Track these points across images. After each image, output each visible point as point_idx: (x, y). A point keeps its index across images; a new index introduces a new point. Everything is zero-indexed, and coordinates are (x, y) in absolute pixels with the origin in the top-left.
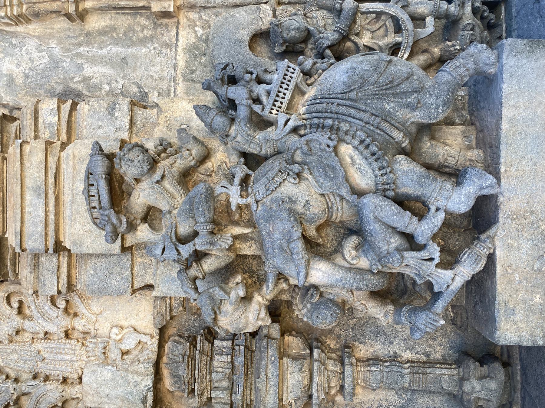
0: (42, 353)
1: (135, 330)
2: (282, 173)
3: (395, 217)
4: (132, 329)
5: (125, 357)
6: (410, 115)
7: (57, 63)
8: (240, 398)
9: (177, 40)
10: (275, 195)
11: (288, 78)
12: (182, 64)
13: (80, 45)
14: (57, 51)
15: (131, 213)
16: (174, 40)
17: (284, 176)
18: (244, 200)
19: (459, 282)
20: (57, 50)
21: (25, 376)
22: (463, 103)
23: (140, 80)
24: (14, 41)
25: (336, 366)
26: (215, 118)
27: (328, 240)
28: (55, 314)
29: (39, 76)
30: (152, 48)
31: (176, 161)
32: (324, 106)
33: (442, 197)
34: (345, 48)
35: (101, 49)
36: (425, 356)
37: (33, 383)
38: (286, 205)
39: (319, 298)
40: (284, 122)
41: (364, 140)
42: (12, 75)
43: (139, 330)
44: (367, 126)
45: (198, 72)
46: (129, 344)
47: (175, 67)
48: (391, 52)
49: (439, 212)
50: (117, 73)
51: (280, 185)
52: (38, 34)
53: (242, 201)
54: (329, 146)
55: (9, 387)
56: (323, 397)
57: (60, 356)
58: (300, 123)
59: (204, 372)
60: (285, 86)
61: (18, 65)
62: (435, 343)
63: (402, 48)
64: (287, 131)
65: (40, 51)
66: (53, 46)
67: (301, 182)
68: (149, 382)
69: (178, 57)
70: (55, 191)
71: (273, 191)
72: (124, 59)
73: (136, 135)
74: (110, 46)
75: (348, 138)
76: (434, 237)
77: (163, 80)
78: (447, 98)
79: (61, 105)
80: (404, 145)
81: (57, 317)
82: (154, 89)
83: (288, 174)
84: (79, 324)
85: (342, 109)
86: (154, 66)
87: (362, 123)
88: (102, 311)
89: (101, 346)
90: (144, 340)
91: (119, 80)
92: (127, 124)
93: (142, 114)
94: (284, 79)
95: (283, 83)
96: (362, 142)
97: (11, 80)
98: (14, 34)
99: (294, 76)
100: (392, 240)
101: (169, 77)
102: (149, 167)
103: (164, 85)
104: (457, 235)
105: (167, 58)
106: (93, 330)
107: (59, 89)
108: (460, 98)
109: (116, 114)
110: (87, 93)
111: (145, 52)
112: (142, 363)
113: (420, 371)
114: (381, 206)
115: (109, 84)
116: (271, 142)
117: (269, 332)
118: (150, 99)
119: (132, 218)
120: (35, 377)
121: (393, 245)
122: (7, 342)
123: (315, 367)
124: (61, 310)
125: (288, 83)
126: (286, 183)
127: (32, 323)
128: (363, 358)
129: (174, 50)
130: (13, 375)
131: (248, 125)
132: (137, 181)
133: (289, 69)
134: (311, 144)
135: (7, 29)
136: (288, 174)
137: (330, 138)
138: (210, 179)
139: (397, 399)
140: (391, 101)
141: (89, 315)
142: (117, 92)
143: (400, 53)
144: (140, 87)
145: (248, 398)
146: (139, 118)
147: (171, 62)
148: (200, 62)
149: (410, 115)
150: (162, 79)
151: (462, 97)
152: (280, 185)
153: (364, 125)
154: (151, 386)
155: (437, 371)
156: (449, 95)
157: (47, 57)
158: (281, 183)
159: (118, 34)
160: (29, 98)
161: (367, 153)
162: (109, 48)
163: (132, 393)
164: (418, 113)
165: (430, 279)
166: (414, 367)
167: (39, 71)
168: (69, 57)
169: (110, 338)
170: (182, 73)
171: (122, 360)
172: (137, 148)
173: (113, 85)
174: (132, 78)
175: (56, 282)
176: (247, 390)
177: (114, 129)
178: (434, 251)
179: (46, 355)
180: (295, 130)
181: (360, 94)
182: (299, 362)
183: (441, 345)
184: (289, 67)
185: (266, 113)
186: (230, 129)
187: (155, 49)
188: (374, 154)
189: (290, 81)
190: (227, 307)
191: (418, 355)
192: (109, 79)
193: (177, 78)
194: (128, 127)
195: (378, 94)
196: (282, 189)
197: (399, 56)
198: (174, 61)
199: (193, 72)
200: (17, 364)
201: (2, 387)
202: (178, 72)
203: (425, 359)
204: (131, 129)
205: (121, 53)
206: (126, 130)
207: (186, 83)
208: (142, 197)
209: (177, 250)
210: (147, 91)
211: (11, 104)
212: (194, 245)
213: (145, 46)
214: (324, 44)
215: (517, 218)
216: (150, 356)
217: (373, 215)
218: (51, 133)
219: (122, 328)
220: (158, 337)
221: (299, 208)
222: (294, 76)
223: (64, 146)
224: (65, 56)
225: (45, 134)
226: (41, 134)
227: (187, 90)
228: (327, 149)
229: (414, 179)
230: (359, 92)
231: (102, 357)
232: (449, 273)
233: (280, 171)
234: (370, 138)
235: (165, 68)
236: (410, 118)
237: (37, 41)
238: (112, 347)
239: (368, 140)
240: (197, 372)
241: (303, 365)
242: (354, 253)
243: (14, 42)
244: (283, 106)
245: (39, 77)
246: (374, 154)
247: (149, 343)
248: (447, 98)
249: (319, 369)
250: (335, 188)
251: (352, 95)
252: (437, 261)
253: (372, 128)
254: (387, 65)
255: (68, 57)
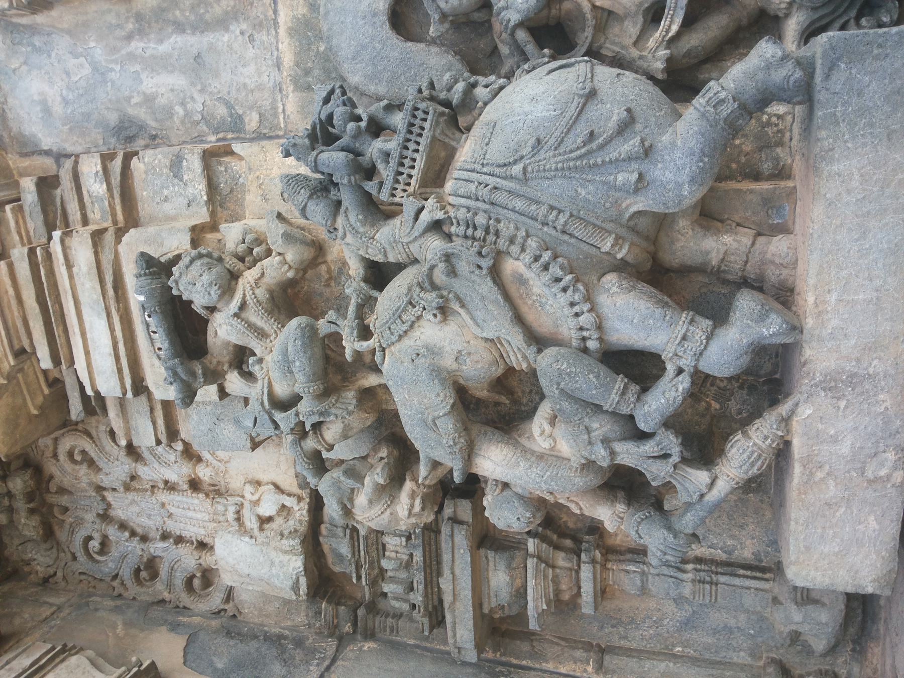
0: (167, 506)
1: (277, 487)
2: (414, 307)
3: (594, 392)
4: (272, 487)
5: (266, 526)
6: (628, 202)
7: (102, 74)
8: (421, 599)
9: (275, 12)
10: (407, 342)
11: (416, 130)
12: (288, 59)
13: (129, 37)
14: (99, 53)
15: (212, 355)
16: (271, 12)
17: (417, 311)
18: (365, 344)
19: (722, 487)
20: (99, 51)
21: (152, 534)
22: (778, 131)
23: (229, 93)
24: (37, 41)
25: (571, 560)
26: (309, 204)
27: (523, 392)
28: (172, 457)
29: (83, 101)
30: (238, 32)
31: (263, 274)
32: (473, 187)
33: (685, 352)
34: (563, 12)
35: (161, 41)
36: (725, 552)
37: (161, 545)
38: (422, 360)
39: (502, 490)
40: (412, 214)
41: (541, 256)
42: (46, 101)
43: (282, 487)
44: (546, 229)
45: (316, 72)
46: (268, 508)
47: (278, 65)
48: (650, 16)
49: (680, 378)
50: (193, 84)
51: (412, 326)
52: (65, 26)
53: (364, 345)
54: (479, 267)
55: (135, 547)
56: (545, 607)
57: (190, 514)
58: (440, 215)
59: (374, 554)
60: (412, 146)
61: (51, 83)
62: (744, 533)
63: (666, 11)
64: (421, 230)
65: (76, 57)
66: (92, 44)
67: (449, 318)
68: (297, 563)
69: (280, 46)
70: (119, 308)
71: (400, 337)
72: (198, 57)
73: (221, 207)
74: (174, 36)
75: (515, 249)
76: (668, 424)
77: (263, 89)
78: (698, 167)
79: (108, 163)
80: (619, 256)
81: (176, 462)
82: (251, 108)
83: (424, 309)
84: (204, 473)
85: (500, 197)
86: (244, 66)
87: (536, 224)
88: (230, 458)
89: (232, 509)
90: (288, 504)
91: (196, 95)
92: (203, 193)
93: (226, 171)
94: (411, 132)
95: (409, 140)
96: (537, 259)
97: (47, 110)
98: (33, 30)
99: (427, 125)
100: (595, 425)
101: (271, 84)
102: (219, 292)
103: (266, 99)
104: (745, 392)
105: (265, 49)
106: (222, 483)
107: (113, 118)
108: (774, 119)
109: (186, 177)
110: (153, 124)
111: (229, 41)
112: (287, 538)
113: (708, 579)
114: (569, 374)
115: (183, 104)
116: (400, 246)
117: (455, 511)
118: (247, 127)
119: (215, 363)
120: (165, 536)
121: (597, 433)
122: (122, 489)
123: (529, 566)
124: (179, 453)
125: (418, 139)
126: (422, 322)
127: (146, 468)
128: (620, 546)
129: (274, 33)
130: (139, 530)
131: (360, 217)
132: (212, 309)
133: (416, 113)
134: (454, 260)
135: (24, 21)
136: (424, 309)
137: (480, 253)
138: (328, 290)
139: (676, 610)
140: (589, 181)
141: (215, 462)
142: (196, 118)
143: (662, 23)
144: (229, 106)
145: (435, 597)
146: (222, 179)
147: (272, 55)
148: (318, 51)
149: (628, 202)
150: (260, 87)
151: (779, 117)
152: (412, 326)
153: (540, 226)
154: (302, 569)
155: (737, 581)
156: (702, 161)
157: (87, 65)
158: (413, 322)
159: (182, 11)
160: (75, 138)
161: (546, 277)
162: (172, 40)
163: (278, 576)
164: (643, 199)
165: (672, 481)
166: (700, 571)
167: (81, 92)
168: (117, 63)
169: (243, 497)
170: (290, 75)
171: (261, 529)
172: (199, 263)
173: (189, 106)
174: (216, 91)
175: (152, 430)
176: (432, 589)
177: (186, 202)
178: (671, 442)
179: (173, 510)
180: (436, 226)
181: (530, 169)
182: (507, 554)
183: (753, 538)
184: (417, 109)
185: (384, 196)
186: (334, 220)
187: (242, 33)
188: (558, 280)
189: (420, 135)
190: (361, 500)
191: (713, 551)
192: (182, 95)
193: (284, 87)
194: (205, 198)
195: (563, 169)
196: (416, 333)
197: (661, 28)
198: (275, 53)
199: (307, 72)
200: (139, 518)
201: (128, 547)
202: (285, 74)
203: (724, 557)
204: (211, 200)
205: (191, 46)
206: (203, 203)
207: (299, 94)
208: (223, 331)
209: (275, 422)
210: (240, 112)
211: (55, 149)
212: (297, 414)
213: (227, 29)
214: (509, 20)
215: (836, 387)
216: (298, 528)
217: (557, 389)
218: (103, 211)
219: (259, 483)
220: (308, 500)
221: (448, 362)
222: (427, 125)
223: (120, 233)
224: (112, 61)
225: (95, 214)
226: (90, 216)
227: (303, 108)
228: (477, 271)
229: (635, 321)
230: (530, 163)
231: (235, 524)
232: (701, 477)
233: (411, 303)
234: (549, 253)
235: (264, 68)
236: (628, 206)
237: (67, 37)
238: (246, 513)
239: (546, 256)
240: (362, 553)
241: (513, 558)
242: (547, 427)
243: (37, 44)
244: (413, 181)
245: (83, 101)
246: (558, 280)
247: (296, 508)
248: (698, 167)
249: (537, 569)
250: (503, 331)
251: (517, 169)
252: (675, 459)
253: (553, 232)
254: (584, 105)
255: (115, 62)
